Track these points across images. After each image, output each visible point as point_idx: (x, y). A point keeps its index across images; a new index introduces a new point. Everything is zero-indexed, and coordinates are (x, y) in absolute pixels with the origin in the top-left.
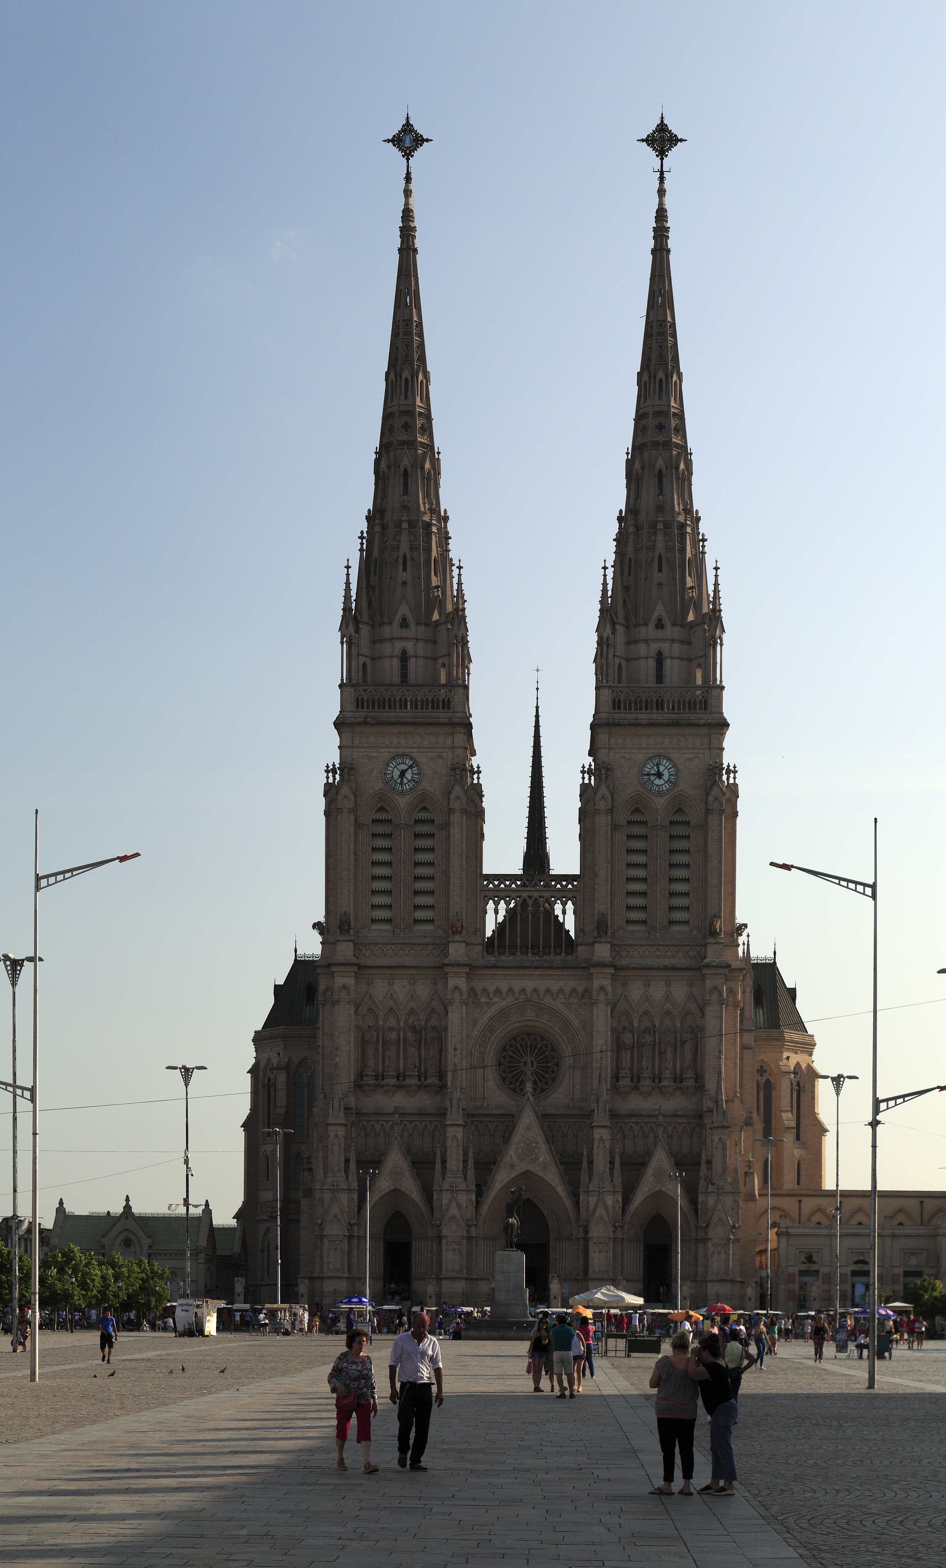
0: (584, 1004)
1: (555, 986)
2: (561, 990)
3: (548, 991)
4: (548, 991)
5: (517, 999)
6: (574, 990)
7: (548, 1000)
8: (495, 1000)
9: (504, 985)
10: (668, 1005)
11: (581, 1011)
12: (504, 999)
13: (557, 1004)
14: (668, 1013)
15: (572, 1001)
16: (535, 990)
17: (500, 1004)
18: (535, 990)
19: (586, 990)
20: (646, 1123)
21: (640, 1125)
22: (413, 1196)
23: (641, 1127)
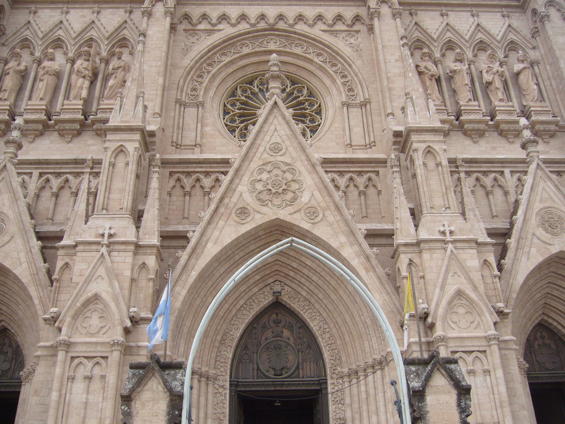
0: (358, 32)
1: (310, 12)
2: (320, 17)
3: (300, 18)
4: (300, 18)
5: (253, 25)
6: (339, 18)
7: (301, 27)
8: (220, 27)
9: (234, 12)
10: (480, 35)
11: (352, 41)
12: (234, 25)
13: (317, 31)
14: (482, 46)
15: (337, 27)
16: (281, 17)
17: (227, 31)
18: (281, 17)
19: (357, 18)
20: (485, 173)
21: (475, 175)
22: (17, 271)
23: (477, 179)
